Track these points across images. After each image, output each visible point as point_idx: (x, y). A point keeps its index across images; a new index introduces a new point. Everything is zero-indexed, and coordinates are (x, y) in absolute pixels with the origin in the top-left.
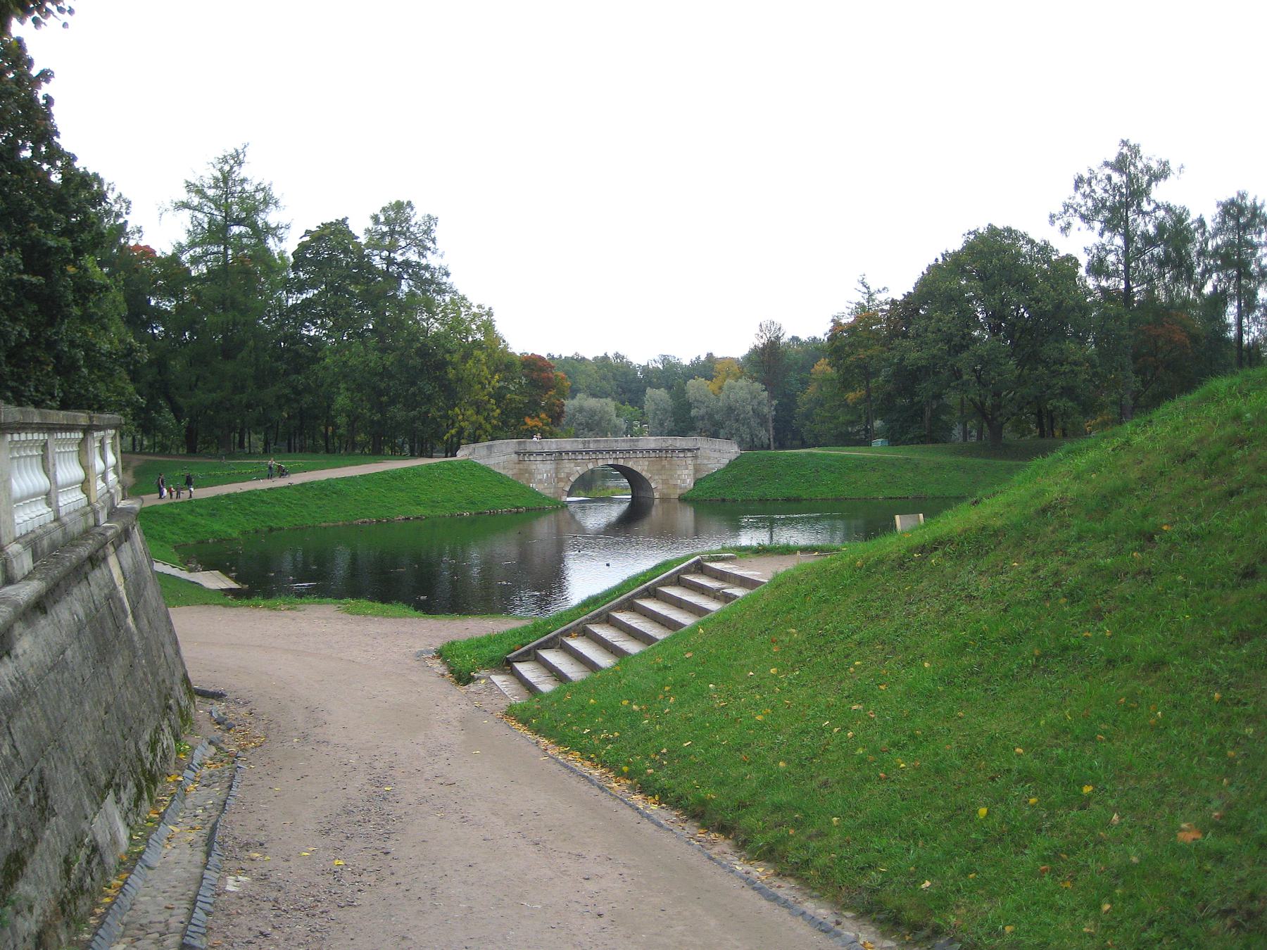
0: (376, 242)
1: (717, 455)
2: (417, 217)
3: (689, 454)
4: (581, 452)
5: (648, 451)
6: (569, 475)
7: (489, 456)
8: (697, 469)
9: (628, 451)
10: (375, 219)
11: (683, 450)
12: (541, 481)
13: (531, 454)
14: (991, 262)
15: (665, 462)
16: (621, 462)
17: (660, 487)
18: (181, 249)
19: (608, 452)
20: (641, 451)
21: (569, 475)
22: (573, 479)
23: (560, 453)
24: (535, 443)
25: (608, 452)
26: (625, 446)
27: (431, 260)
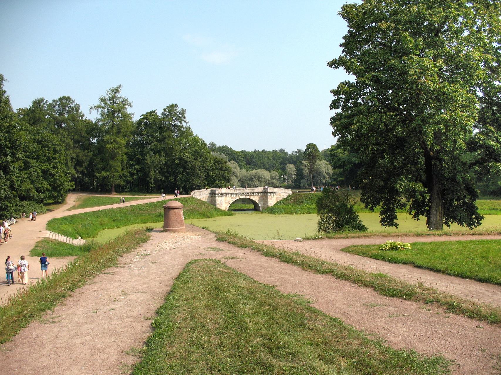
0: (165, 116)
2: (179, 109)
4: (233, 194)
10: (164, 110)
14: (333, 121)
16: (248, 197)
18: (98, 120)
21: (229, 202)
27: (184, 124)
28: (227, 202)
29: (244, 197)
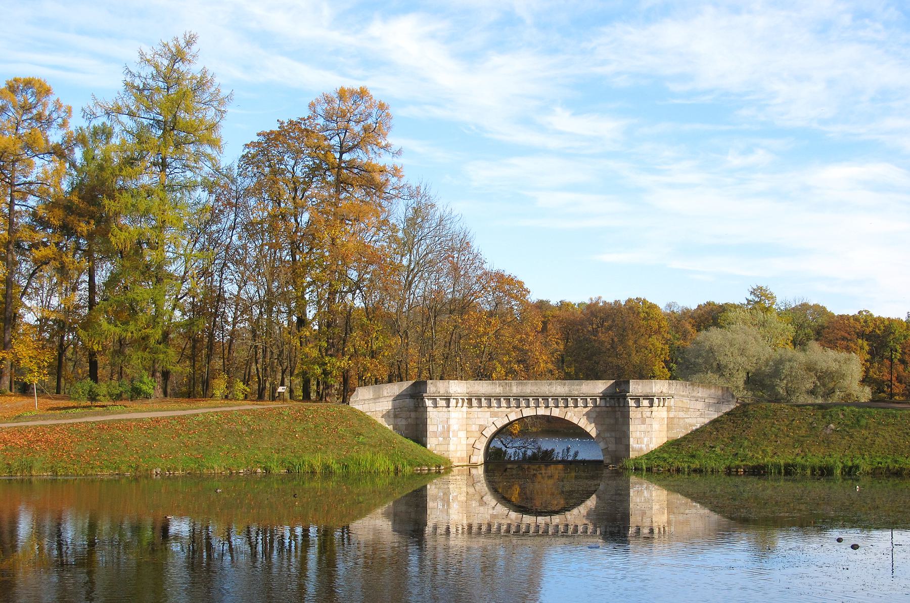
12: (435, 434)
22: (489, 433)
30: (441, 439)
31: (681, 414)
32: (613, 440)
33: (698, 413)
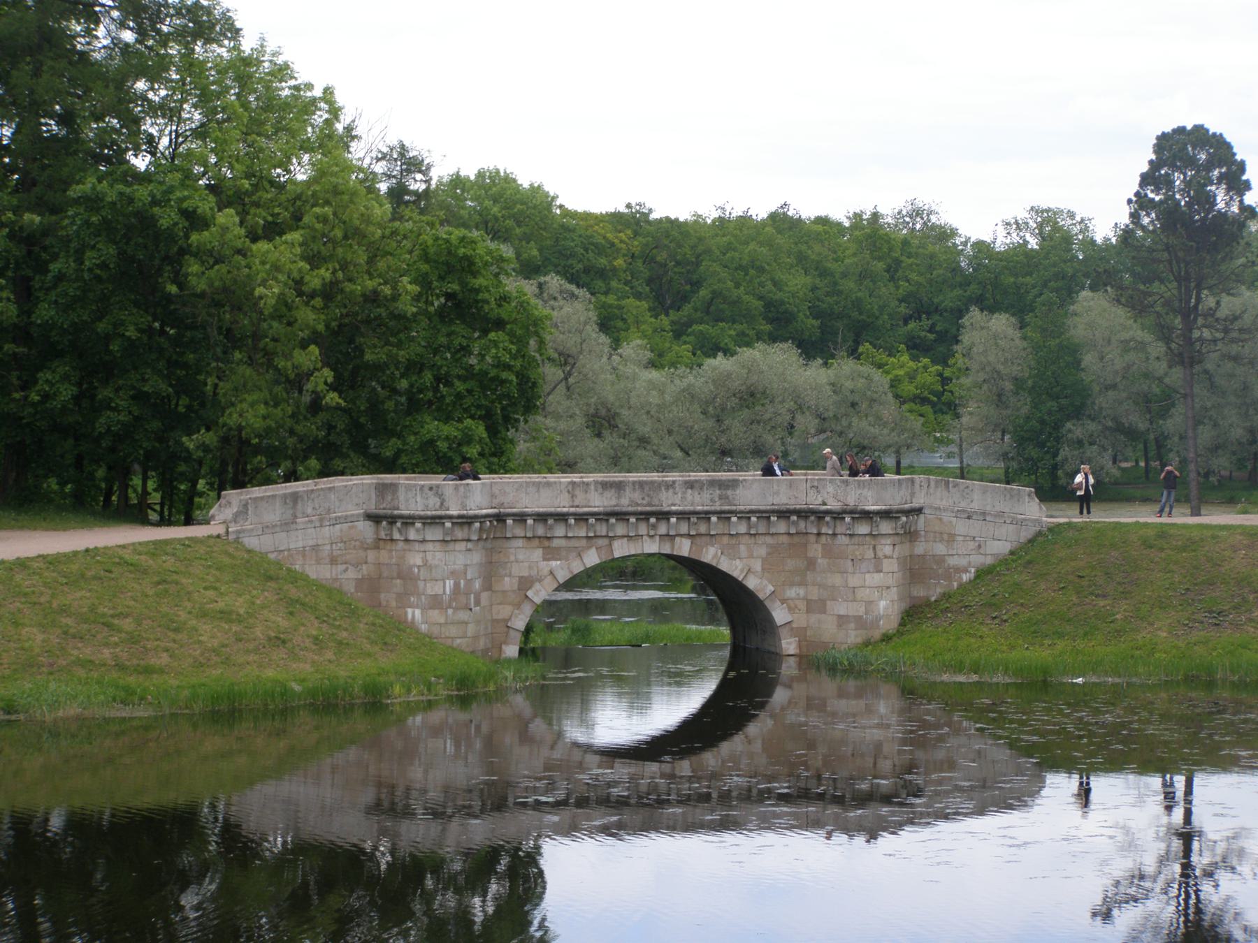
1: (974, 528)
3: (886, 527)
4: (561, 517)
5: (764, 515)
6: (526, 583)
7: (288, 525)
8: (915, 571)
9: (705, 516)
11: (866, 516)
12: (436, 602)
13: (409, 521)
15: (815, 550)
16: (684, 548)
17: (801, 620)
19: (644, 516)
20: (745, 516)
21: (526, 583)
22: (540, 593)
23: (500, 518)
24: (416, 492)
25: (644, 516)
26: (699, 501)
28: (509, 583)
29: (651, 547)
30: (450, 611)
31: (940, 549)
32: (802, 605)
33: (972, 545)
